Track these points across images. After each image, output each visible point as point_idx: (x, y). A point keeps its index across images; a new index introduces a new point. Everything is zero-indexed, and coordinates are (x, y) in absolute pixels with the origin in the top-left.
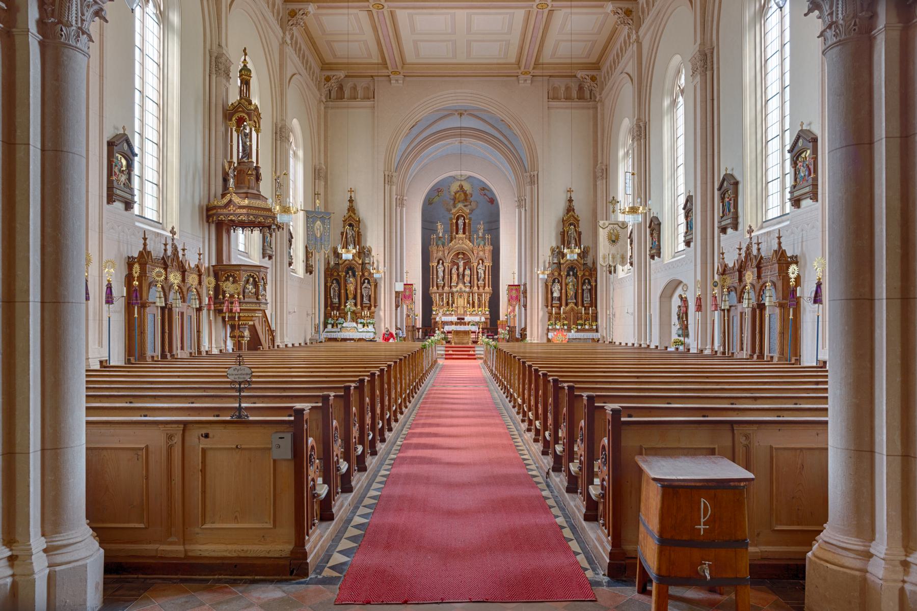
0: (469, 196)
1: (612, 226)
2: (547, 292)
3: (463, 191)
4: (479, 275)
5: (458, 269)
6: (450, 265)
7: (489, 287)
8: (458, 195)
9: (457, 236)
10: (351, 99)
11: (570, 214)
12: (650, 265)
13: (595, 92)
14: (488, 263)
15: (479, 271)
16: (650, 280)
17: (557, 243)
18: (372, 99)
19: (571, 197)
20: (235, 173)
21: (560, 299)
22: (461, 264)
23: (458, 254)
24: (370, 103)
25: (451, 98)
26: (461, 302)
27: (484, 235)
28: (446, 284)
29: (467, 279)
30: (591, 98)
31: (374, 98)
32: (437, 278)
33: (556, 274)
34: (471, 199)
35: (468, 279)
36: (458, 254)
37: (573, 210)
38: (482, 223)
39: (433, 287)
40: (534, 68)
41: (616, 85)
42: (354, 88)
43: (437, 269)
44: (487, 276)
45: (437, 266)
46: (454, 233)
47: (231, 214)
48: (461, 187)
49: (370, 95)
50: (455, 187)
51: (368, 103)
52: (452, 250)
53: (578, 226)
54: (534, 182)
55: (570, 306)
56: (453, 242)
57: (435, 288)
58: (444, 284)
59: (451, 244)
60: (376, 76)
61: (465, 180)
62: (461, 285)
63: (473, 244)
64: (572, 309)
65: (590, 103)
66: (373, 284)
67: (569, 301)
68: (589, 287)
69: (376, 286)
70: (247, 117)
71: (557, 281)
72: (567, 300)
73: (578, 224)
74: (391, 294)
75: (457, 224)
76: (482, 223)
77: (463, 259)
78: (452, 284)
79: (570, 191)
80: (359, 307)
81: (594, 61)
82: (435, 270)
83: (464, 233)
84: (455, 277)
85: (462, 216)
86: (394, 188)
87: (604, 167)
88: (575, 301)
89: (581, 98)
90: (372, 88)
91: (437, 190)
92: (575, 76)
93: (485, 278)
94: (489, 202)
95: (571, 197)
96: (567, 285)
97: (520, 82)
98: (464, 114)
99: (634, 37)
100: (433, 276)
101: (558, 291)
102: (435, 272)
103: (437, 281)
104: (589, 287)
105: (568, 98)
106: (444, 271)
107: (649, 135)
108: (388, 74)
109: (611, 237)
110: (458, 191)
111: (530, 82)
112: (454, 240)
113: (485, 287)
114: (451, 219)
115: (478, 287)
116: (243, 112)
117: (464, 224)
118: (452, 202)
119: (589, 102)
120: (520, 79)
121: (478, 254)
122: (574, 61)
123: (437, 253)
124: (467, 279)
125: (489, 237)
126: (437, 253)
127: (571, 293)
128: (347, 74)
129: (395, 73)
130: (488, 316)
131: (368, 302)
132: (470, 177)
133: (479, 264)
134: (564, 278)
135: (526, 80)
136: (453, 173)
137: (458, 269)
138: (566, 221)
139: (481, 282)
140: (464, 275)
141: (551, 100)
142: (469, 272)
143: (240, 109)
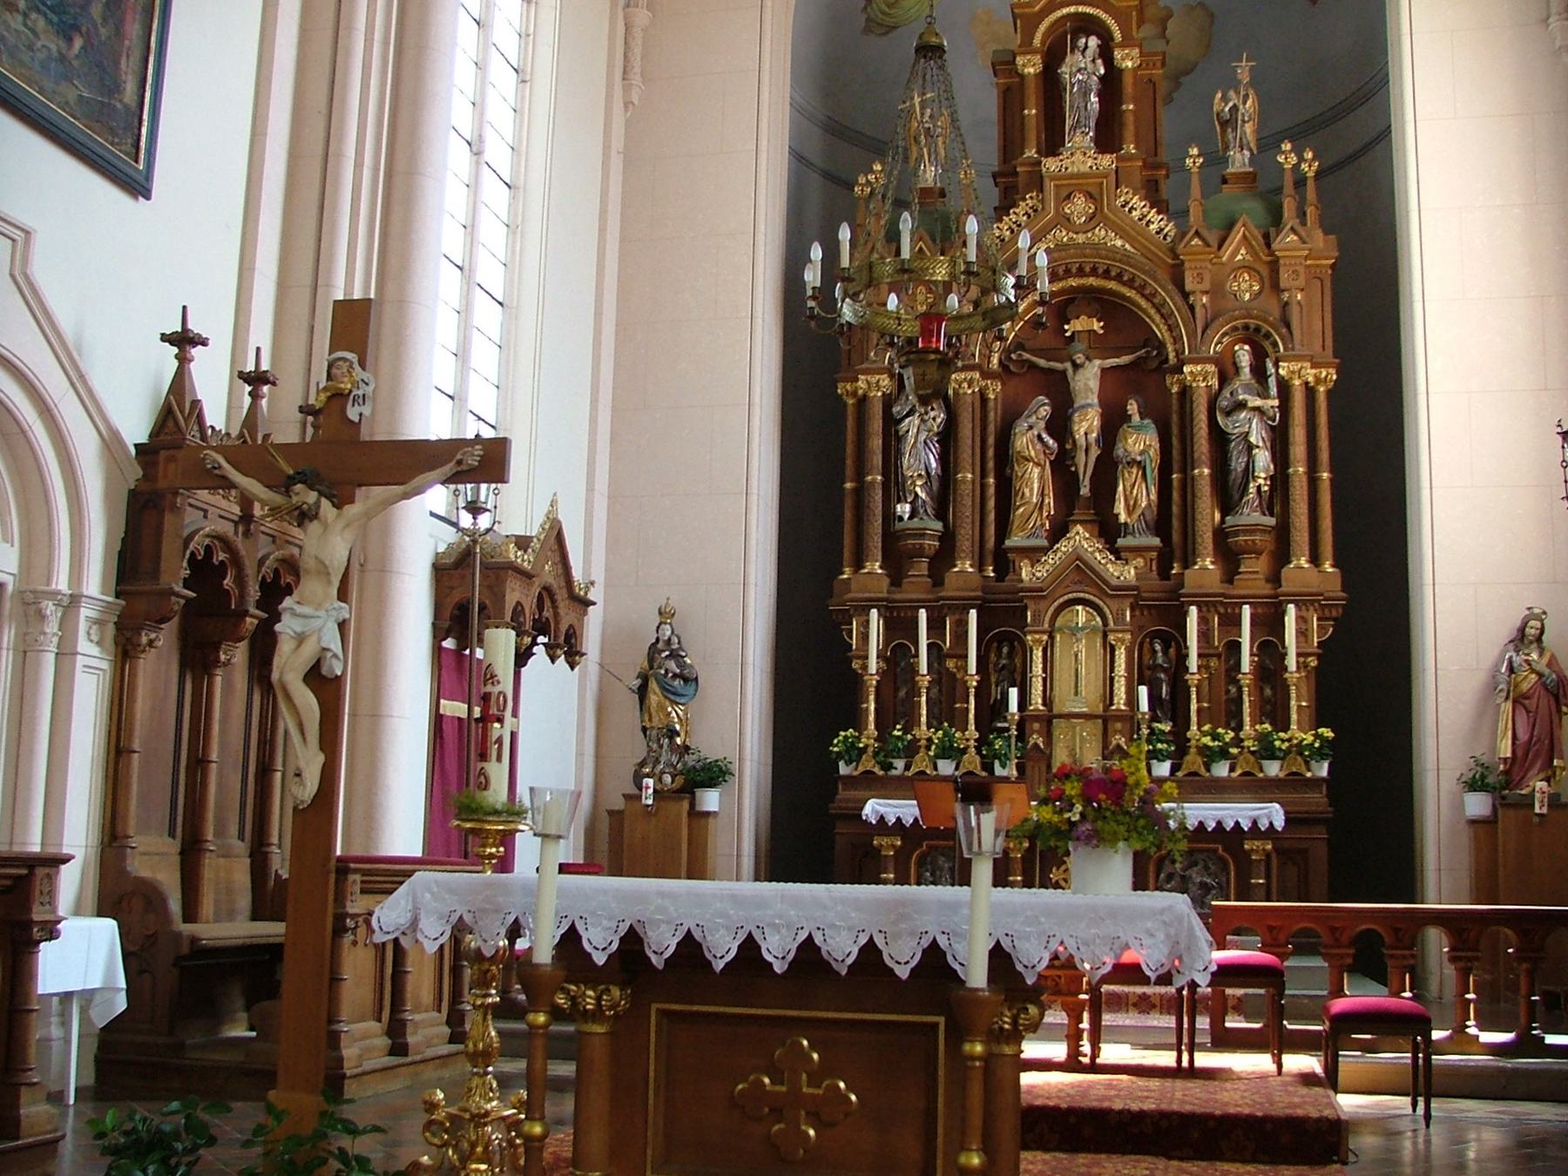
4: (1238, 463)
5: (1060, 425)
6: (994, 389)
7: (1315, 559)
9: (1051, 165)
15: (1233, 425)
22: (1088, 381)
27: (1267, 145)
32: (895, 486)
35: (1146, 496)
38: (1243, 70)
39: (858, 565)
43: (891, 423)
44: (1299, 469)
45: (888, 402)
46: (1031, 153)
57: (875, 567)
58: (948, 539)
62: (1081, 539)
63: (1178, 215)
75: (1050, 80)
77: (1099, 346)
78: (1014, 541)
82: (876, 424)
83: (1107, 139)
84: (1034, 482)
85: (1086, 25)
93: (1280, 479)
100: (860, 475)
102: (876, 443)
103: (889, 517)
106: (947, 439)
112: (1030, 200)
113: (1282, 555)
115: (1229, 556)
117: (1111, 84)
125: (1310, 169)
130: (1317, 800)
137: (1060, 425)
139: (1251, 515)
140: (1108, 468)
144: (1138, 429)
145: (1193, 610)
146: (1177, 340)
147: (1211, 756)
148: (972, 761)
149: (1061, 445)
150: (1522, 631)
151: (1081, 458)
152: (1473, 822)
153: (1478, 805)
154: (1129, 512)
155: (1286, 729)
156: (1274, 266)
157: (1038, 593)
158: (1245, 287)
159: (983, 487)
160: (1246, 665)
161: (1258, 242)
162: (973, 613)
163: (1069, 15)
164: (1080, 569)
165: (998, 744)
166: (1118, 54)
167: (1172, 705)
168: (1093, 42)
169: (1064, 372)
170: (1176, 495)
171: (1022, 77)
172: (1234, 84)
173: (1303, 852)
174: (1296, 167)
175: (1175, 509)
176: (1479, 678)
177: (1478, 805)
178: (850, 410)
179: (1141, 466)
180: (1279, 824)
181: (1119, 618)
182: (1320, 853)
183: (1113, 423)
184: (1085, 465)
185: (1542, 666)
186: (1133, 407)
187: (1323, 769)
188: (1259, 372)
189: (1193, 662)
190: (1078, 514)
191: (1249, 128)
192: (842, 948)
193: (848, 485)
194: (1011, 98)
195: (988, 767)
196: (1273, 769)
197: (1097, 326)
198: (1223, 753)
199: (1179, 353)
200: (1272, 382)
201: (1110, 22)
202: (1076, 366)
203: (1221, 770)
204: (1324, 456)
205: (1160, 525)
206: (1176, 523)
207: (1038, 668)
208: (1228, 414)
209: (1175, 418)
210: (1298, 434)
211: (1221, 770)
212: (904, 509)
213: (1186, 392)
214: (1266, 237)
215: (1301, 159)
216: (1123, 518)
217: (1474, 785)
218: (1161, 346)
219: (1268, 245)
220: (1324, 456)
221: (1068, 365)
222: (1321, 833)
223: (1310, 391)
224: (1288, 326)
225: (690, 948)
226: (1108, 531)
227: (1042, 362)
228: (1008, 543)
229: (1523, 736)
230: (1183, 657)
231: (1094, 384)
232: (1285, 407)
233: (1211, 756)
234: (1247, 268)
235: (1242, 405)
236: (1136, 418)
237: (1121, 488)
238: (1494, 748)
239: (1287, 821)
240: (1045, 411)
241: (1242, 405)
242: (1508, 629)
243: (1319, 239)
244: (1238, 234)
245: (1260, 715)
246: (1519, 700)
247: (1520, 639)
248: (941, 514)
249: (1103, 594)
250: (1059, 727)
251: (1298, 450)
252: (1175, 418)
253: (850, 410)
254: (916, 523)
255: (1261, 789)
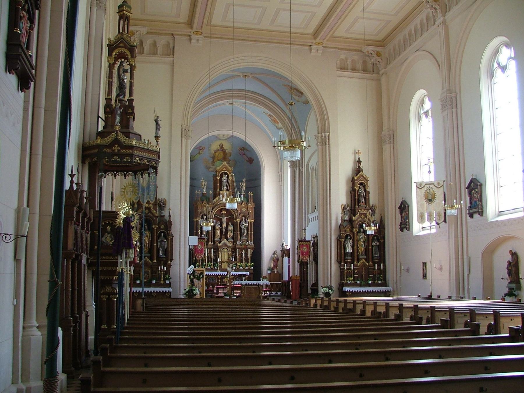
0: (228, 155)
1: (428, 186)
2: (341, 247)
3: (222, 151)
5: (221, 225)
8: (217, 154)
9: (221, 192)
10: (150, 54)
11: (360, 174)
12: (467, 223)
13: (378, 66)
14: (251, 220)
16: (467, 237)
17: (347, 201)
18: (172, 56)
19: (359, 159)
20: (121, 110)
21: (352, 254)
22: (224, 220)
23: (221, 210)
24: (169, 59)
25: (246, 61)
26: (224, 255)
28: (210, 240)
29: (230, 235)
30: (374, 71)
31: (173, 55)
33: (348, 230)
34: (230, 158)
36: (221, 210)
37: (362, 171)
38: (244, 180)
40: (327, 41)
41: (408, 61)
42: (155, 44)
44: (250, 232)
46: (218, 190)
47: (116, 155)
48: (221, 146)
49: (171, 51)
50: (215, 146)
51: (169, 59)
52: (216, 206)
53: (368, 185)
54: (325, 143)
55: (363, 260)
56: (217, 198)
58: (208, 240)
59: (215, 200)
60: (177, 35)
61: (226, 139)
64: (364, 265)
65: (374, 75)
66: (170, 238)
67: (360, 257)
68: (378, 244)
69: (172, 239)
70: (128, 53)
71: (349, 238)
72: (358, 256)
73: (367, 184)
74: (185, 248)
75: (221, 179)
76: (244, 180)
77: (226, 215)
79: (358, 153)
80: (155, 261)
81: (381, 39)
84: (218, 232)
85: (226, 173)
86: (189, 141)
87: (391, 133)
88: (365, 257)
89: (365, 70)
90: (171, 46)
91: (199, 149)
92: (361, 51)
94: (248, 162)
95: (359, 159)
96: (358, 241)
97: (312, 51)
98: (248, 76)
99: (439, 20)
101: (350, 247)
104: (378, 244)
105: (354, 70)
107: (461, 103)
108: (189, 34)
109: (428, 197)
110: (218, 150)
111: (321, 52)
114: (215, 176)
116: (125, 47)
118: (211, 160)
119: (372, 74)
120: (313, 48)
121: (241, 210)
122: (367, 37)
123: (202, 208)
124: (230, 235)
125: (252, 195)
126: (202, 208)
127: (362, 249)
128: (150, 31)
129: (196, 33)
130: (252, 271)
131: (165, 257)
132: (232, 137)
133: (242, 220)
134: (356, 234)
135: (318, 50)
136: (215, 133)
137: (221, 225)
138: (357, 180)
141: (339, 70)
142: (232, 228)
143: (122, 45)
144: (231, 226)
145: (238, 249)
146: (236, 216)
147: (240, 266)
148: (212, 267)
149: (221, 227)
150: (274, 252)
151: (223, 229)
152: (269, 274)
153: (269, 272)
154: (230, 236)
155: (248, 263)
156: (248, 207)
157: (220, 247)
158: (244, 210)
159: (212, 233)
160: (244, 256)
161: (246, 204)
162: (212, 249)
163: (224, 172)
164: (225, 244)
165: (216, 265)
166: (229, 178)
167: (236, 260)
168: (226, 176)
169: (221, 218)
170: (235, 235)
171: (217, 179)
172: (242, 182)
173: (250, 277)
174: (251, 195)
175: (235, 236)
176: (269, 258)
177: (269, 272)
178: (195, 224)
179: (231, 231)
180: (249, 274)
181: (230, 250)
182: (252, 277)
183: (227, 225)
184: (224, 230)
185: (276, 257)
186: (230, 223)
187: (252, 268)
188: (246, 221)
189: (238, 255)
190: (223, 236)
191: (244, 188)
192: (255, 284)
193: (195, 232)
194: (215, 181)
195: (214, 267)
196: (247, 268)
197: (225, 212)
198: (241, 266)
199: (236, 217)
200: (247, 222)
201: (229, 174)
202: (223, 218)
203: (241, 268)
204: (252, 230)
205: (233, 238)
206: (235, 238)
207: (220, 256)
208: (242, 225)
209: (235, 225)
210: (250, 228)
211: (241, 268)
212: (203, 236)
213: (236, 222)
214: (247, 203)
215: (251, 193)
216: (229, 237)
217: (269, 270)
218: (233, 215)
219: (247, 205)
220: (252, 230)
221: (222, 218)
222: (252, 275)
223: (251, 223)
224: (249, 215)
225: (249, 284)
226: (227, 239)
227: (219, 217)
228: (215, 240)
229: (274, 264)
230: (236, 254)
231: (225, 220)
232: (248, 225)
233: (240, 266)
234: (244, 207)
235: (244, 225)
236: (230, 225)
237: (228, 234)
238: (271, 265)
239: (250, 274)
240: (219, 223)
241: (244, 225)
242: (273, 252)
243: (253, 204)
244: (243, 204)
245: (246, 262)
246: (274, 260)
247: (274, 253)
248: (207, 236)
249: (228, 247)
250: (222, 263)
251: (250, 230)
252: (235, 225)
253: (195, 224)
254: (204, 237)
255: (246, 270)
